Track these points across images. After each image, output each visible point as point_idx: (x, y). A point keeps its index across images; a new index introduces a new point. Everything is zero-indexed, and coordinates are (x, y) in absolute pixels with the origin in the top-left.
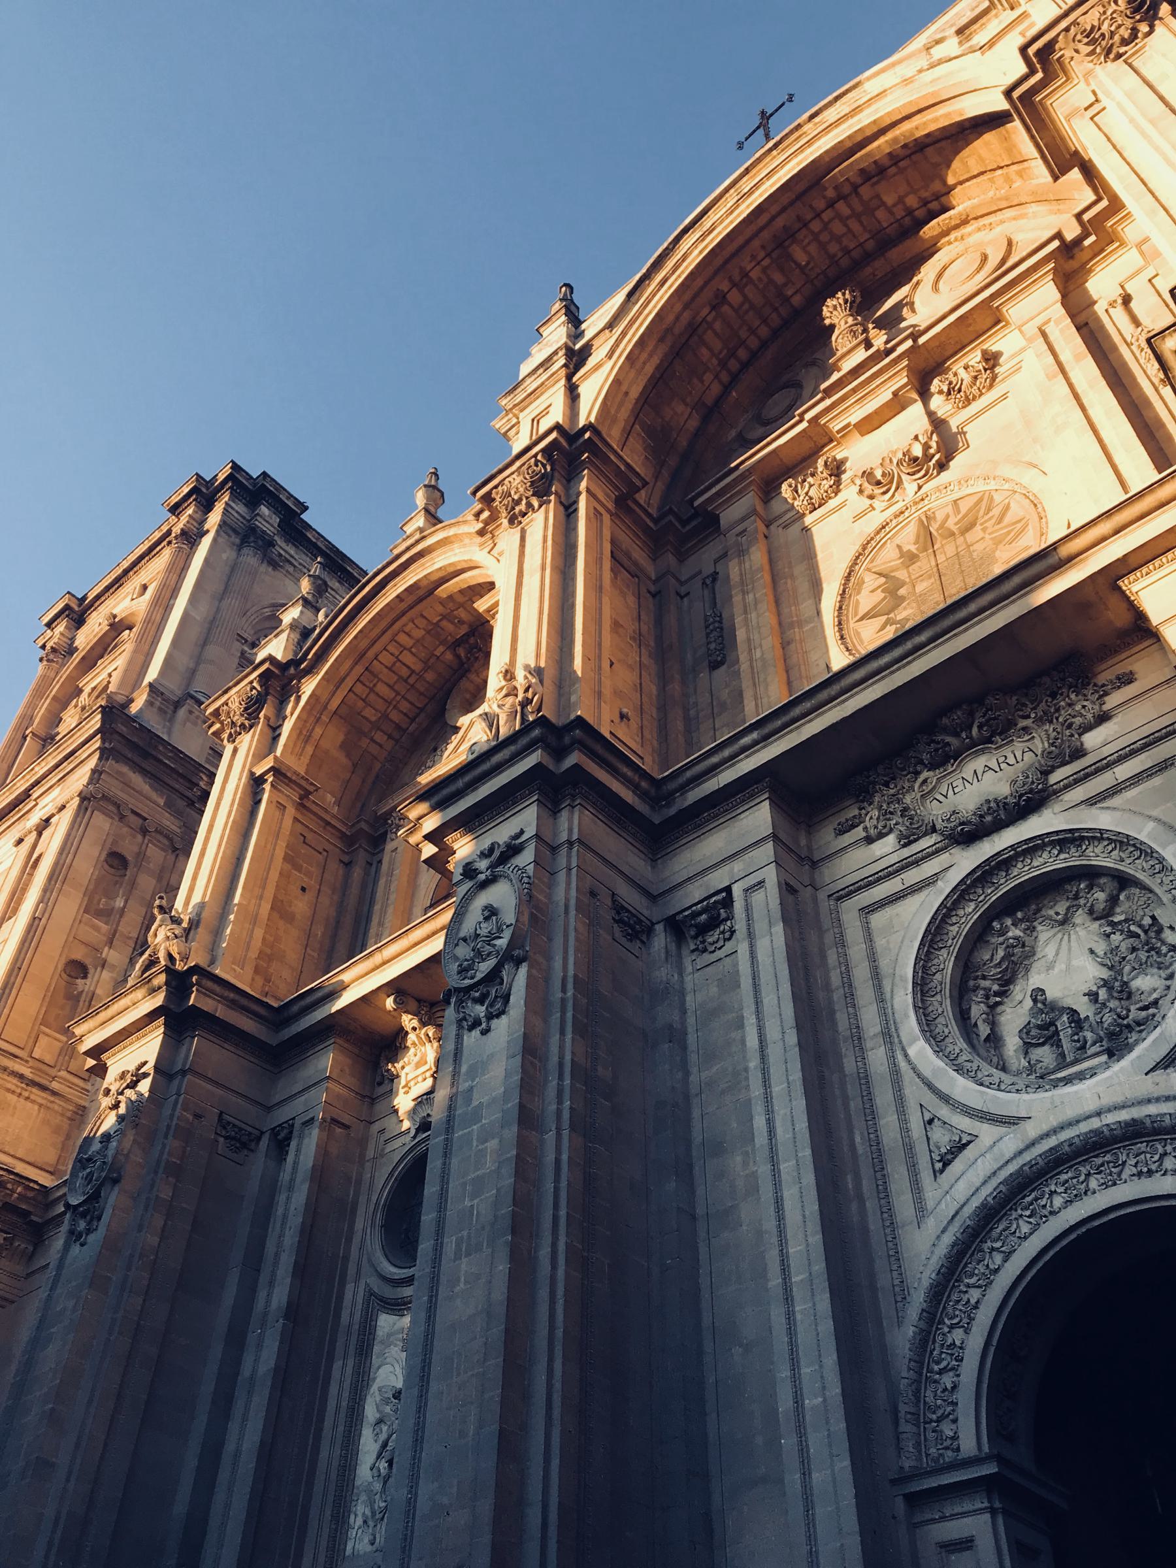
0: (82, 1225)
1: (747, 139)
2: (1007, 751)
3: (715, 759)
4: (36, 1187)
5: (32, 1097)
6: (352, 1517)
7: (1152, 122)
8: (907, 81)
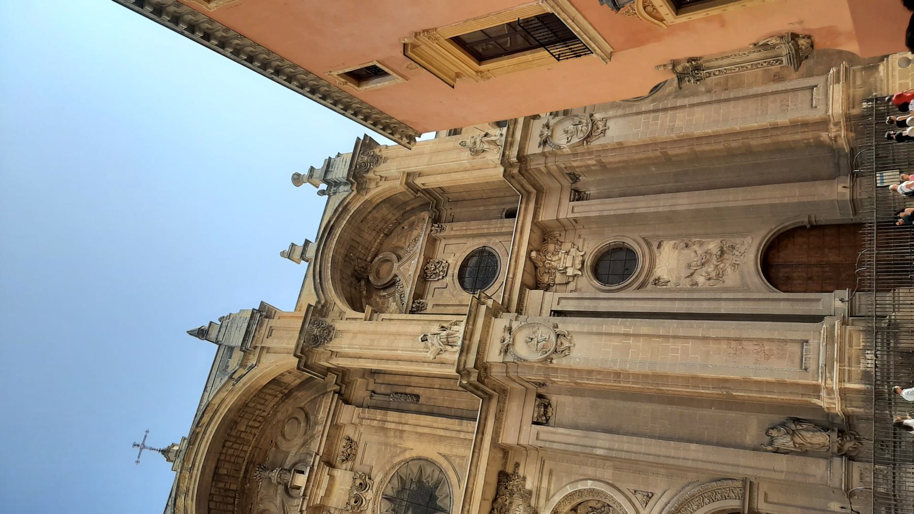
1: (139, 457)
7: (369, 346)
8: (232, 391)
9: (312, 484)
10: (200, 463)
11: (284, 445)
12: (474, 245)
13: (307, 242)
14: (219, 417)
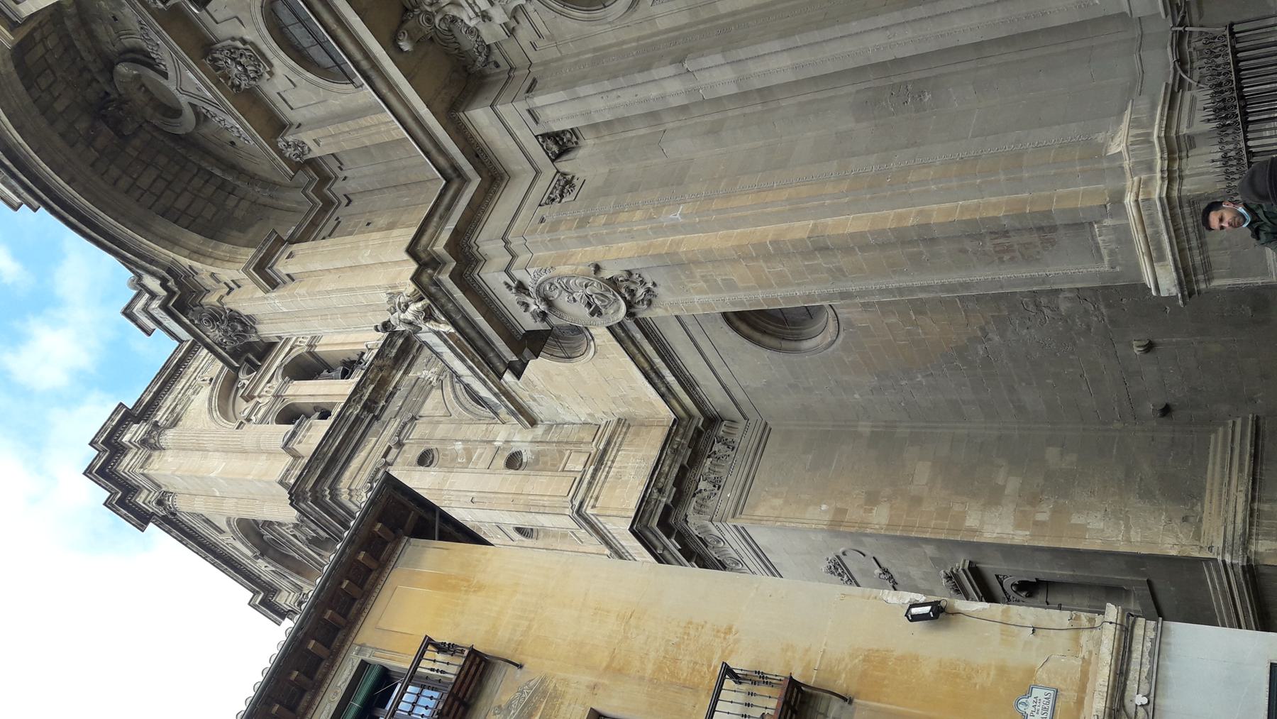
0: (641, 292)
4: (675, 428)
5: (611, 458)
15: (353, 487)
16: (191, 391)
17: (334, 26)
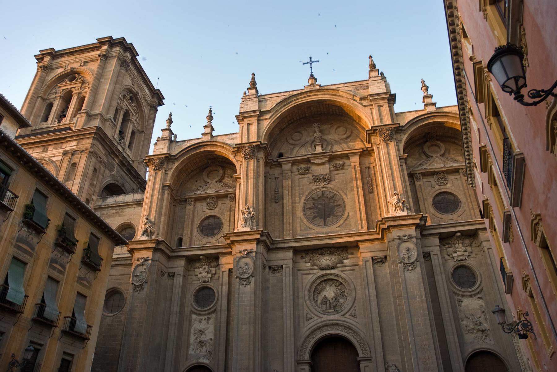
0: (138, 289)
2: (332, 257)
3: (285, 241)
6: (190, 348)
8: (347, 98)
9: (319, 155)
10: (311, 99)
11: (333, 131)
12: (461, 196)
13: (435, 104)
14: (334, 98)
15: (94, 146)
16: (133, 77)
17: (210, 248)
